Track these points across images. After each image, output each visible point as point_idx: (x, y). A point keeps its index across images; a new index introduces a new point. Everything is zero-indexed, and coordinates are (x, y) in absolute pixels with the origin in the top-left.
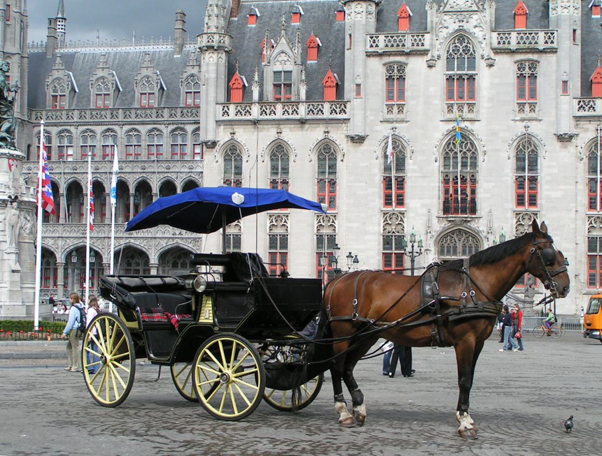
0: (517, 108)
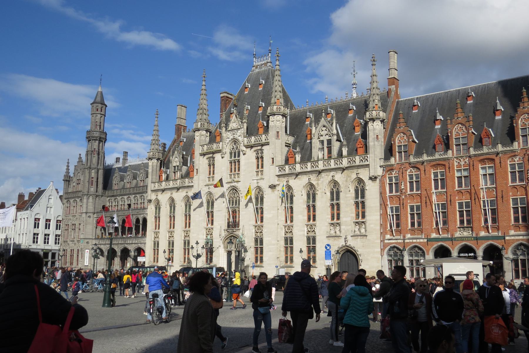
0: (255, 174)
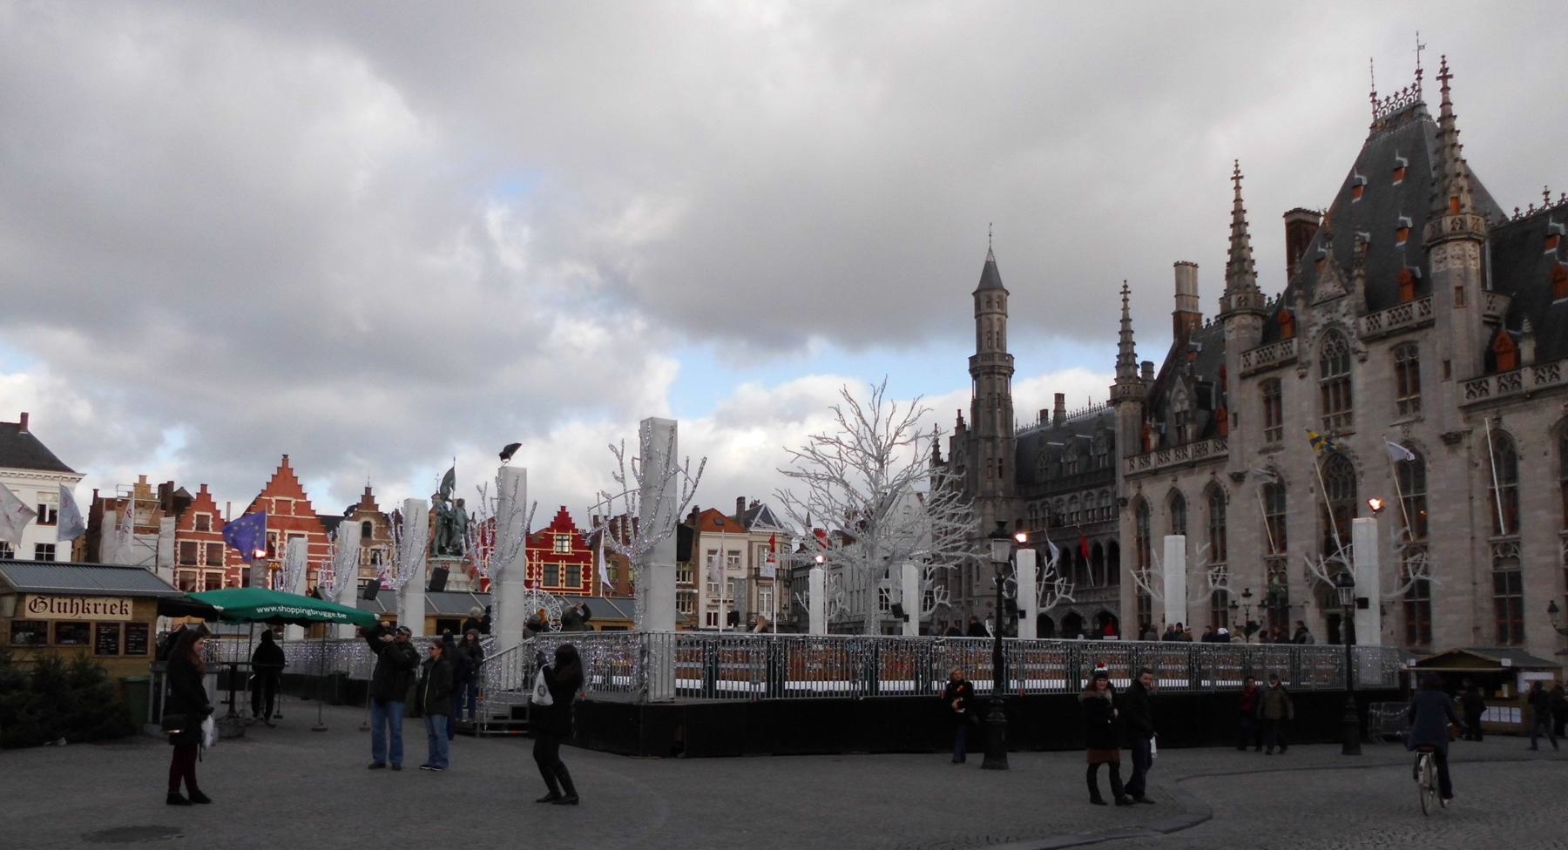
0: (1397, 408)
